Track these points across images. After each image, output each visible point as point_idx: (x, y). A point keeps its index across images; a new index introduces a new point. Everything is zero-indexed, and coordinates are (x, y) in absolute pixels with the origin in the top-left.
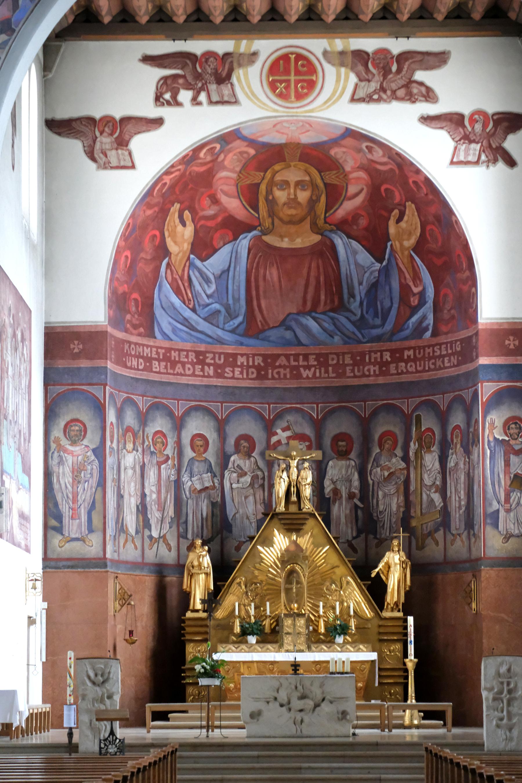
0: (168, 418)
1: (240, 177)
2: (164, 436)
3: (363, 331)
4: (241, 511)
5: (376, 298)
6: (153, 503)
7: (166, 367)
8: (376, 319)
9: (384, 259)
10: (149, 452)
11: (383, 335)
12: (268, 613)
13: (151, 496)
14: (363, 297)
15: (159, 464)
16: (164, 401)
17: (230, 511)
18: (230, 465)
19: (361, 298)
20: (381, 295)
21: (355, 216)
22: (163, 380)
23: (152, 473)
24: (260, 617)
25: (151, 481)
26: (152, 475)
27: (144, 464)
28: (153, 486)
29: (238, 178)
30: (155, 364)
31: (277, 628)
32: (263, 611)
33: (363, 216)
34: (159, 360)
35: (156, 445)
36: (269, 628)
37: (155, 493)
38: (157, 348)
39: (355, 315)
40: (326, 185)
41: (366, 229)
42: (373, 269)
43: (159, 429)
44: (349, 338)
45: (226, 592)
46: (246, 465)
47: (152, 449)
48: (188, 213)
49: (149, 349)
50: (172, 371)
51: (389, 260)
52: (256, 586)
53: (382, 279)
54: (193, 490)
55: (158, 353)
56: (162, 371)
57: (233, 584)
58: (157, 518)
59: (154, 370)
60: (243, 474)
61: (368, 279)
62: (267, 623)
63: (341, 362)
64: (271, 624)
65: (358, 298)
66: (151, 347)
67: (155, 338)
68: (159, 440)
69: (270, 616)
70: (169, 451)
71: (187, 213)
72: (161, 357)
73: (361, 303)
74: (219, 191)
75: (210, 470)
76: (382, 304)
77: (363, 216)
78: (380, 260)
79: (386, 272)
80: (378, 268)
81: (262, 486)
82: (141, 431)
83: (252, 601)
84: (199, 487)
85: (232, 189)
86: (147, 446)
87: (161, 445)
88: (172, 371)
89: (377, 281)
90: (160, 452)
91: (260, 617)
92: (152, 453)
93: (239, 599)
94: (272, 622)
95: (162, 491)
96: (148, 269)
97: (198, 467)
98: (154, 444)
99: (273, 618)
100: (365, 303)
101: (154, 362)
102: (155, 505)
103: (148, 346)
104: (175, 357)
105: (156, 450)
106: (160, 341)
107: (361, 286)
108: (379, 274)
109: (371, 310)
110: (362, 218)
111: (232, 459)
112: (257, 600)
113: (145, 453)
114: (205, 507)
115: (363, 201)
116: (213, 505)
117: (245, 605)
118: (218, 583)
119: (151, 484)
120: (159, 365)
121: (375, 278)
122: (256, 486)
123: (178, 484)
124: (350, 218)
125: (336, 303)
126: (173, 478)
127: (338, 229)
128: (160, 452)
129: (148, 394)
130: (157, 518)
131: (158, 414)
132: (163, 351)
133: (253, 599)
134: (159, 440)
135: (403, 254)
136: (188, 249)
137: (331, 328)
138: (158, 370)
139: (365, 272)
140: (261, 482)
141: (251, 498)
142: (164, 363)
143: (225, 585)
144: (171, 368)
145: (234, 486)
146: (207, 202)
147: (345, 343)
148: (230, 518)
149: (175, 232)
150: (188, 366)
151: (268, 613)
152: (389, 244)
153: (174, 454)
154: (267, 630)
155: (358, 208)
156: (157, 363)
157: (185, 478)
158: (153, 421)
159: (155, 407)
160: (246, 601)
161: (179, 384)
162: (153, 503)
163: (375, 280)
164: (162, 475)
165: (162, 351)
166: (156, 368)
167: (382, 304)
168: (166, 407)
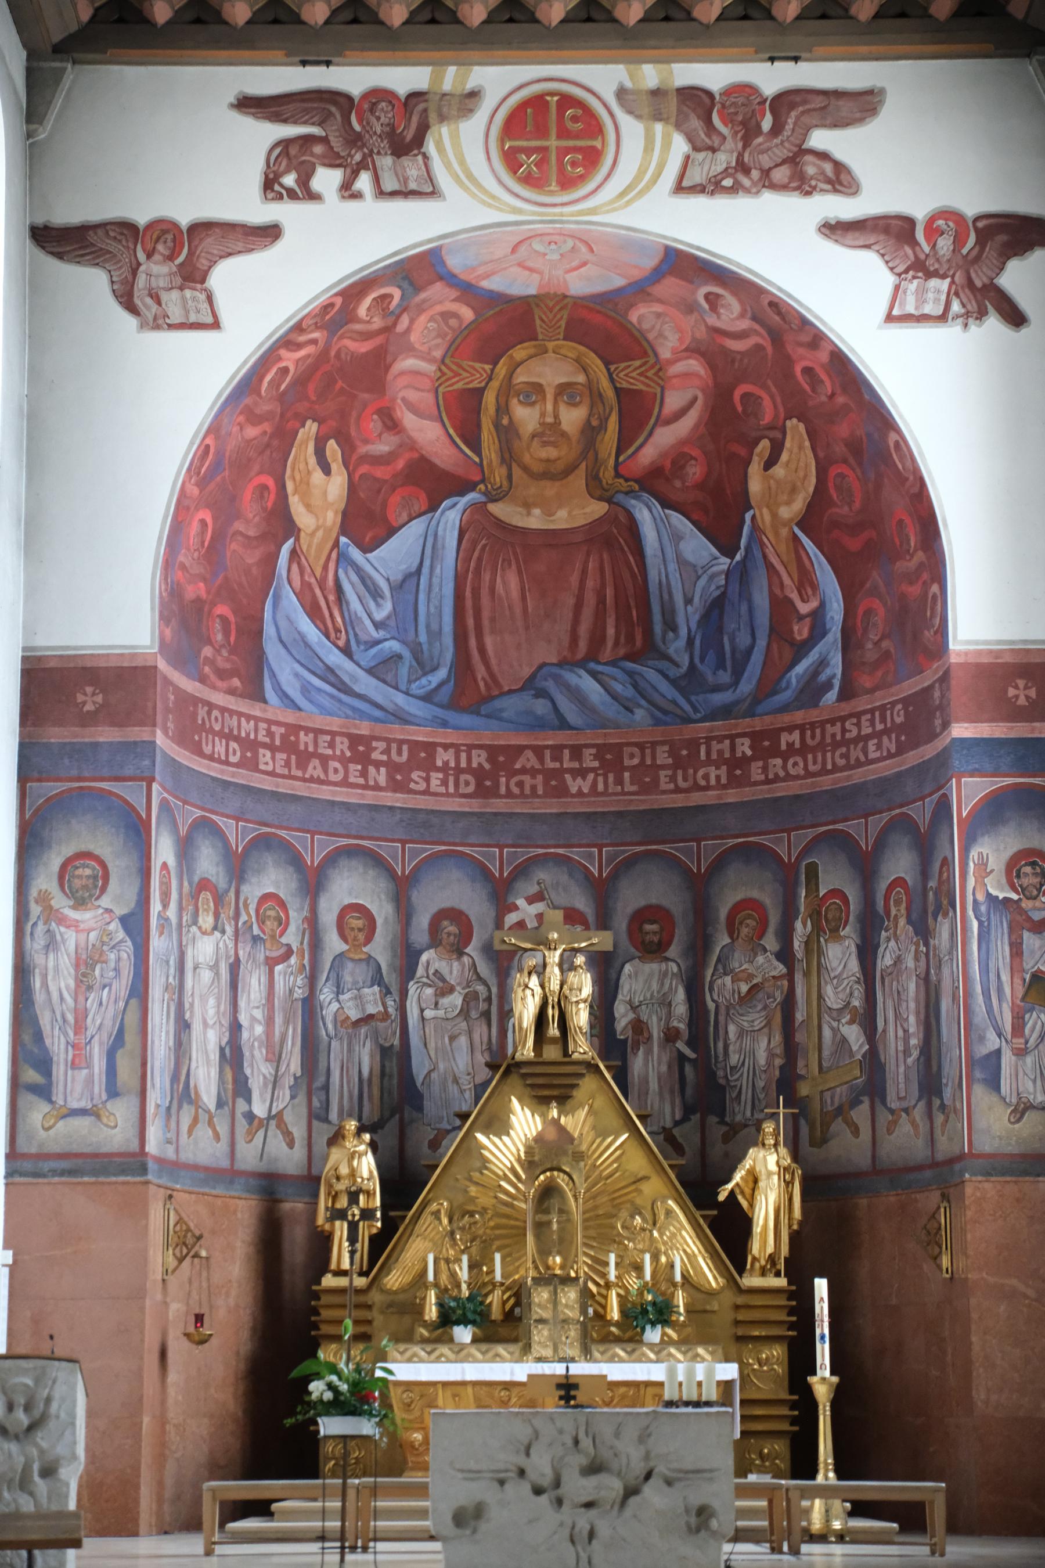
0: (291, 869)
1: (443, 374)
2: (282, 904)
3: (693, 698)
5: (720, 630)
6: (256, 1044)
7: (287, 764)
8: (721, 672)
9: (739, 548)
10: (248, 937)
11: (736, 703)
12: (498, 1277)
13: (252, 1028)
14: (694, 626)
15: (271, 963)
16: (283, 833)
19: (689, 630)
20: (730, 625)
21: (678, 459)
22: (280, 790)
23: (254, 982)
24: (481, 1287)
25: (252, 997)
26: (254, 985)
27: (237, 960)
28: (258, 1007)
29: (439, 374)
30: (265, 755)
31: (517, 1310)
32: (488, 1273)
33: (696, 459)
34: (272, 748)
35: (263, 923)
36: (500, 1310)
37: (260, 1023)
38: (270, 722)
39: (677, 665)
40: (618, 391)
41: (701, 486)
42: (715, 569)
43: (271, 890)
44: (665, 712)
45: (410, 1228)
47: (256, 931)
48: (336, 447)
49: (252, 723)
50: (299, 774)
51: (748, 549)
52: (472, 1220)
53: (734, 588)
55: (270, 734)
56: (278, 771)
57: (424, 1216)
58: (265, 1077)
59: (262, 767)
61: (704, 590)
62: (495, 1299)
63: (649, 762)
64: (504, 1303)
65: (683, 632)
66: (257, 719)
67: (265, 702)
68: (269, 913)
69: (502, 1284)
71: (332, 445)
72: (278, 742)
73: (690, 642)
74: (399, 401)
76: (732, 640)
77: (696, 459)
78: (728, 551)
79: (741, 575)
80: (726, 567)
82: (233, 890)
83: (463, 1252)
85: (425, 399)
86: (245, 923)
87: (276, 924)
88: (299, 774)
89: (724, 594)
90: (273, 937)
91: (481, 1287)
92: (256, 939)
93: (437, 1247)
94: (505, 1297)
95: (277, 1020)
96: (252, 557)
98: (261, 920)
99: (508, 1289)
100: (698, 643)
101: (261, 751)
102: (260, 1048)
103: (249, 717)
104: (306, 744)
105: (264, 932)
106: (274, 709)
107: (689, 608)
108: (727, 579)
109: (711, 656)
110: (693, 462)
112: (474, 1250)
113: (240, 938)
115: (696, 426)
117: (447, 1261)
118: (392, 1214)
119: (252, 1005)
120: (273, 758)
121: (718, 588)
124: (668, 464)
125: (639, 643)
127: (643, 489)
128: (273, 937)
129: (248, 816)
130: (265, 1077)
131: (269, 859)
132: (283, 730)
133: (467, 1248)
134: (269, 913)
135: (777, 534)
136: (334, 522)
137: (629, 692)
138: (270, 768)
139: (699, 578)
142: (284, 756)
143: (405, 1217)
144: (298, 768)
146: (375, 424)
149: (308, 484)
150: (334, 764)
151: (498, 1277)
152: (748, 516)
153: (302, 943)
154: (496, 1314)
155: (683, 442)
156: (268, 754)
158: (259, 872)
159: (262, 843)
160: (452, 1252)
161: (314, 799)
162: (256, 1044)
163: (718, 593)
164: (277, 986)
165: (278, 731)
166: (267, 763)
167: (732, 640)
168: (286, 846)
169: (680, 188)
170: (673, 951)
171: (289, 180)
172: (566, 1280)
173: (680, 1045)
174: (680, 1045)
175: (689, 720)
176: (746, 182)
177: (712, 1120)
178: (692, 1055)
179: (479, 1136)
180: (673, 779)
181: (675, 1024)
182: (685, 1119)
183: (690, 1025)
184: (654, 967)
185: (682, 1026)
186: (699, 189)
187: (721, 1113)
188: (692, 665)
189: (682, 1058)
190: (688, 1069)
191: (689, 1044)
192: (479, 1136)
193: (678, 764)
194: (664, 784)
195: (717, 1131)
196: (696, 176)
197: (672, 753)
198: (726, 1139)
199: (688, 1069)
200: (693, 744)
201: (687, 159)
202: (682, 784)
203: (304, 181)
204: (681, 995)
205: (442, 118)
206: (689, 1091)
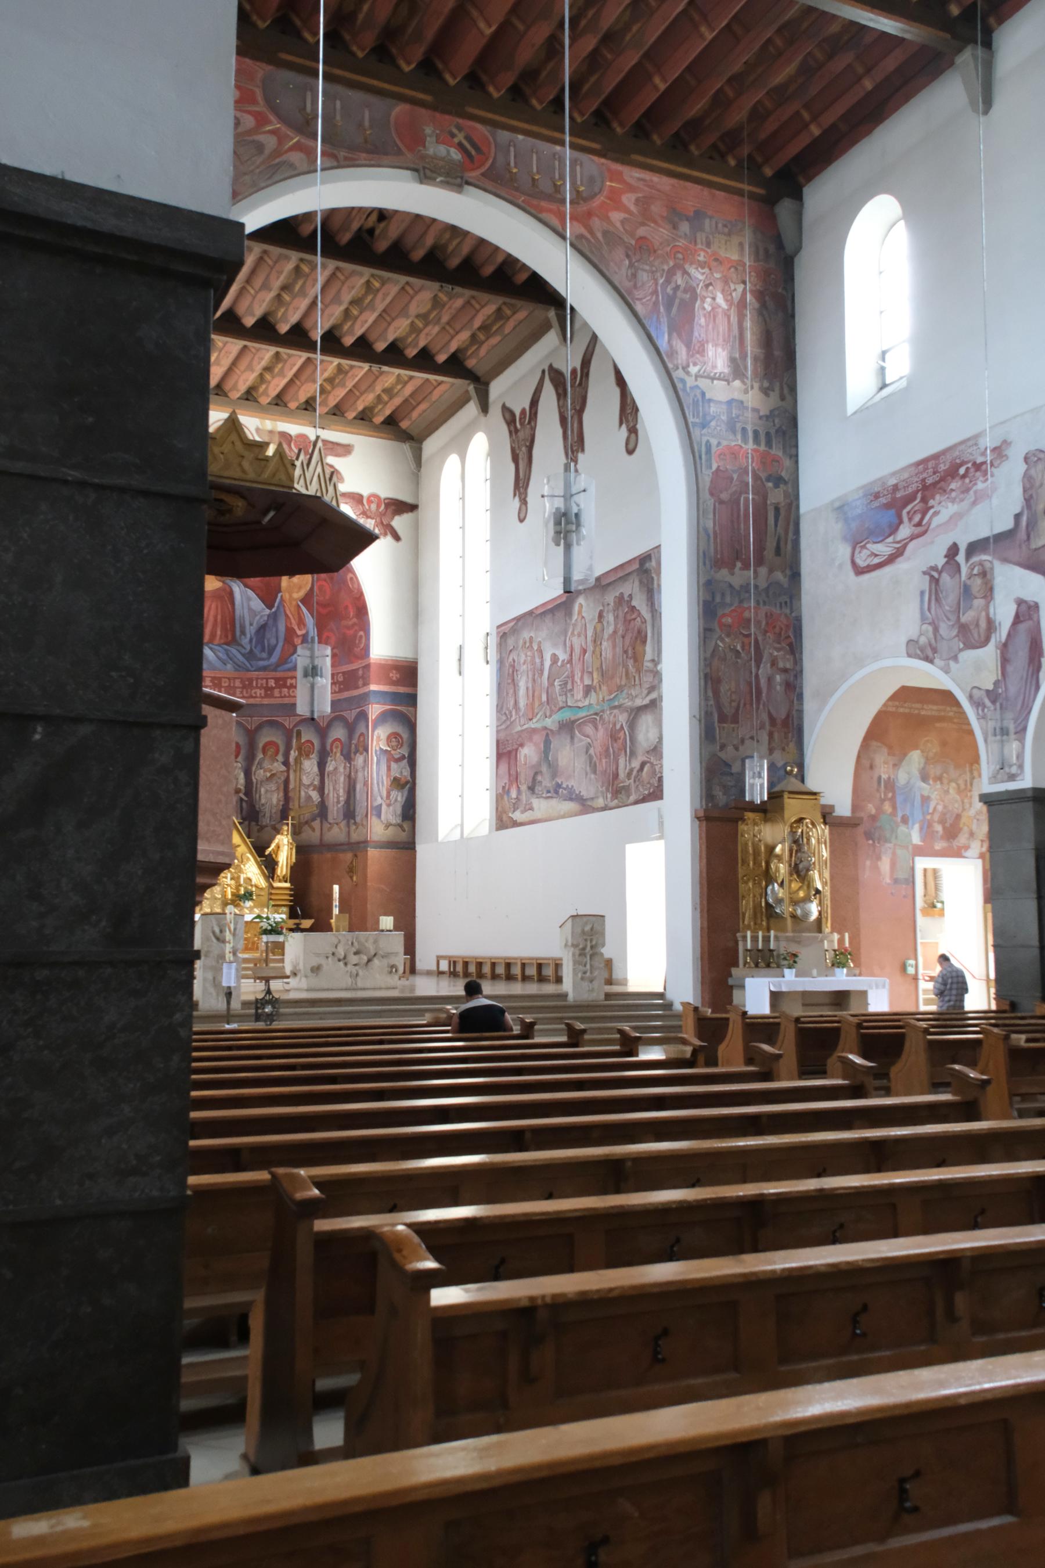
5: (263, 637)
73: (251, 641)
109: (259, 647)
147: (236, 670)
173: (242, 795)
174: (242, 795)
175: (248, 670)
177: (253, 823)
178: (246, 799)
180: (242, 692)
181: (239, 786)
185: (242, 788)
187: (257, 821)
188: (251, 649)
189: (241, 800)
190: (244, 805)
191: (246, 794)
193: (244, 687)
197: (241, 682)
198: (259, 831)
199: (244, 805)
200: (251, 680)
202: (245, 695)
206: (244, 812)
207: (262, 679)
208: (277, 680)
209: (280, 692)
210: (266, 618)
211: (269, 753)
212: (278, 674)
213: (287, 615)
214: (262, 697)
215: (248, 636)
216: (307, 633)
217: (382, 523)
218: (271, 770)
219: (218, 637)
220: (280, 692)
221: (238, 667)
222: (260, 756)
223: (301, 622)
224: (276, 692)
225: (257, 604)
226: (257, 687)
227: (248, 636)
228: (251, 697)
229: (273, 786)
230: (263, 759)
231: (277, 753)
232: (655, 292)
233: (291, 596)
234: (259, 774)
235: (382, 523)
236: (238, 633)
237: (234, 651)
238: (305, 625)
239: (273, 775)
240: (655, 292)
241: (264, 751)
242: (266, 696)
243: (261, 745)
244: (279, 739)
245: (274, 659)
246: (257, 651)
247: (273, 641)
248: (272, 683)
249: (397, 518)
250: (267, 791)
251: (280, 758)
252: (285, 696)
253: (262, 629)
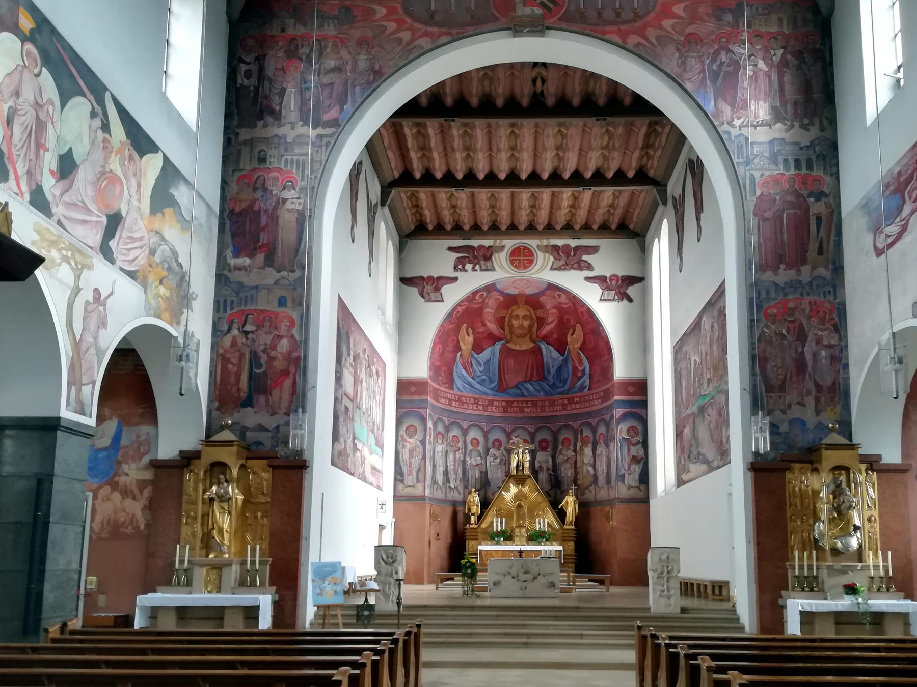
2: (458, 438)
4: (495, 476)
17: (489, 477)
18: (490, 453)
46: (498, 453)
54: (471, 465)
55: (455, 398)
60: (496, 458)
66: (452, 394)
70: (460, 445)
75: (480, 455)
81: (505, 464)
84: (474, 464)
96: (451, 356)
97: (474, 454)
106: (456, 391)
111: (491, 450)
114: (477, 474)
116: (482, 472)
122: (502, 464)
123: (464, 461)
126: (462, 459)
140: (504, 462)
141: (500, 470)
145: (492, 464)
148: (489, 479)
157: (468, 459)
159: (453, 423)
169: (552, 269)
170: (549, 449)
171: (460, 267)
172: (523, 526)
176: (567, 267)
179: (503, 492)
182: (551, 489)
183: (553, 467)
184: (544, 453)
185: (551, 467)
186: (556, 269)
189: (550, 474)
190: (552, 477)
191: (552, 471)
192: (503, 492)
194: (547, 410)
195: (559, 492)
196: (555, 266)
199: (552, 477)
201: (553, 262)
203: (463, 267)
204: (551, 459)
205: (496, 252)
207: (560, 399)
208: (569, 399)
209: (571, 407)
210: (561, 362)
211: (565, 445)
212: (570, 396)
213: (572, 359)
214: (560, 410)
215: (552, 374)
216: (584, 368)
217: (620, 292)
218: (567, 456)
219: (534, 377)
220: (571, 407)
221: (547, 393)
222: (560, 447)
223: (581, 363)
224: (569, 408)
225: (555, 354)
226: (558, 405)
227: (552, 374)
228: (555, 411)
229: (568, 465)
230: (562, 449)
231: (569, 445)
232: (703, 71)
233: (573, 346)
234: (560, 458)
235: (620, 292)
236: (546, 373)
237: (544, 384)
238: (583, 364)
239: (568, 458)
240: (703, 71)
241: (563, 445)
242: (563, 410)
243: (561, 440)
244: (571, 438)
245: (567, 387)
246: (557, 383)
247: (566, 376)
248: (566, 401)
249: (630, 288)
250: (565, 469)
251: (572, 448)
252: (573, 409)
253: (559, 370)
